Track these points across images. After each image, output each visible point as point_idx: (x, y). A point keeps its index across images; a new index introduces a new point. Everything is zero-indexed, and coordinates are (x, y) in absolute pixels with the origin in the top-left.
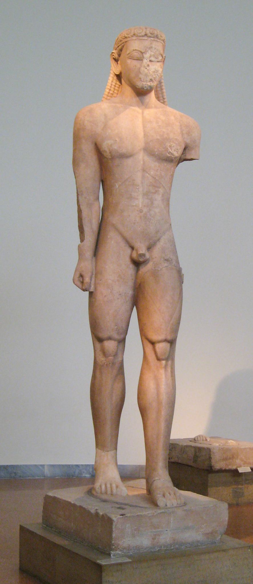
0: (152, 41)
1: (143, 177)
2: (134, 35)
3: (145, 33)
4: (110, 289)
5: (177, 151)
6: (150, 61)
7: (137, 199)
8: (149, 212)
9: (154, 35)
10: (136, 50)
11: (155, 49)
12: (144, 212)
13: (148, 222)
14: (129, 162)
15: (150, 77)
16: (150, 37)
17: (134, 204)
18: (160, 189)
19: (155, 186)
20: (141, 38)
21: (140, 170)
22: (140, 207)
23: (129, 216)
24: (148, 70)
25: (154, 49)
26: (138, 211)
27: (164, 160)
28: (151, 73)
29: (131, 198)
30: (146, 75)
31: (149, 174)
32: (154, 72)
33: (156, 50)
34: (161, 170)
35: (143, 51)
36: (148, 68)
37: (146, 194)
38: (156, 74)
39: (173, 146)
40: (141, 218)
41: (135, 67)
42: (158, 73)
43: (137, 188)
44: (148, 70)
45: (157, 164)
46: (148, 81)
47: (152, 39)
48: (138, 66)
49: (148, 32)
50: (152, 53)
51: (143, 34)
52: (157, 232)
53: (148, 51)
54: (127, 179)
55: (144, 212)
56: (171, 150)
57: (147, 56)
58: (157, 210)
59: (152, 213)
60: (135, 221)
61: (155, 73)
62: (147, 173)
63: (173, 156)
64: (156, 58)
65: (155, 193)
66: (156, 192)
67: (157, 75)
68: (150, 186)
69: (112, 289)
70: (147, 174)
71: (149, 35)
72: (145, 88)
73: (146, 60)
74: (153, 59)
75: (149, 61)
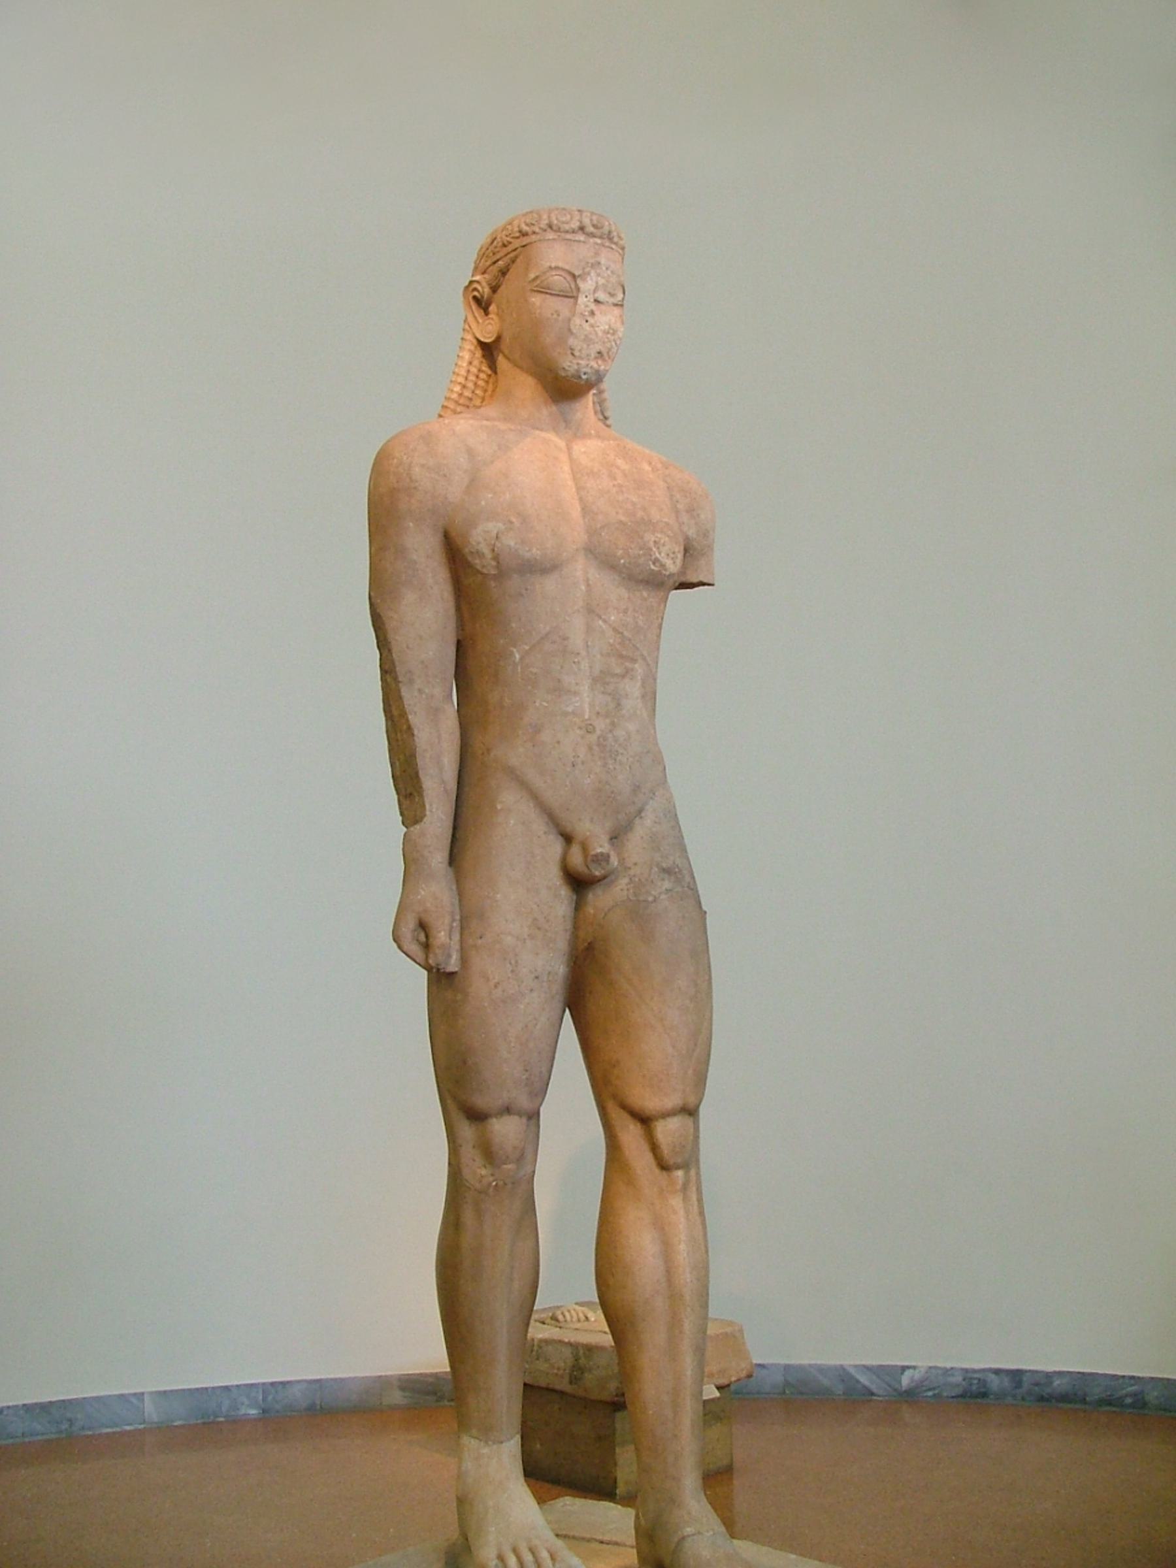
0: (597, 247)
1: (589, 629)
2: (550, 226)
3: (578, 224)
4: (510, 964)
5: (673, 558)
6: (597, 301)
7: (576, 693)
8: (611, 731)
9: (601, 230)
10: (557, 268)
11: (607, 269)
12: (598, 732)
13: (610, 762)
14: (549, 584)
15: (598, 347)
16: (592, 235)
17: (570, 709)
18: (636, 666)
19: (621, 656)
20: (568, 236)
21: (581, 610)
22: (587, 717)
23: (558, 742)
24: (592, 326)
25: (604, 268)
26: (580, 728)
27: (641, 581)
28: (600, 334)
29: (559, 690)
30: (588, 340)
31: (605, 621)
32: (608, 333)
33: (609, 272)
34: (634, 610)
35: (577, 273)
36: (591, 320)
37: (600, 680)
38: (612, 338)
39: (662, 541)
40: (590, 748)
41: (555, 316)
42: (616, 337)
43: (574, 662)
44: (592, 326)
45: (623, 592)
46: (593, 356)
47: (599, 241)
48: (565, 312)
49: (587, 221)
50: (601, 281)
51: (575, 225)
52: (636, 789)
53: (589, 274)
54: (547, 634)
55: (598, 732)
56: (660, 553)
57: (587, 285)
58: (632, 727)
59: (620, 733)
60: (574, 757)
61: (609, 336)
62: (600, 617)
63: (666, 570)
64: (612, 295)
65: (623, 676)
66: (627, 673)
67: (613, 343)
68: (608, 655)
69: (517, 962)
70: (600, 622)
71: (591, 229)
72: (584, 377)
73: (584, 296)
74: (601, 296)
75: (592, 300)
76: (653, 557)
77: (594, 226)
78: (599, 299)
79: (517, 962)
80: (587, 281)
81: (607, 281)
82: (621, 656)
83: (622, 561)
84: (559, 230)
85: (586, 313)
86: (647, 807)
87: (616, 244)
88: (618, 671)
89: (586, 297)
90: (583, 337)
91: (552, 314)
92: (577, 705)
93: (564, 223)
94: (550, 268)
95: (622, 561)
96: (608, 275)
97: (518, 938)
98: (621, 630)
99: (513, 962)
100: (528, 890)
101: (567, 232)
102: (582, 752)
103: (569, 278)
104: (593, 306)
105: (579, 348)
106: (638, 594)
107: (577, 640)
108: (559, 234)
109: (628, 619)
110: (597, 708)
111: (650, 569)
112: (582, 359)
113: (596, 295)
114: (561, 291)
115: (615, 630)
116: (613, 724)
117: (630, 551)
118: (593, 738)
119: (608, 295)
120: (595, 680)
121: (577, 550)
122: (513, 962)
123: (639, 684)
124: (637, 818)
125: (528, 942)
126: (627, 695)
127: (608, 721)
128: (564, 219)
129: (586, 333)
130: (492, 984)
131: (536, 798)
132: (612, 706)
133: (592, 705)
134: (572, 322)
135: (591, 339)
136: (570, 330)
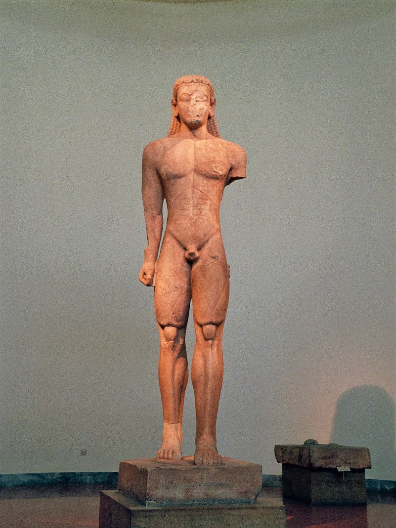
1: (193, 192)
7: (188, 210)
10: (185, 94)
14: (182, 181)
15: (197, 114)
16: (196, 82)
18: (208, 201)
20: (189, 84)
29: (183, 209)
36: (194, 107)
37: (196, 206)
40: (191, 224)
44: (195, 108)
45: (205, 181)
48: (187, 106)
55: (194, 220)
57: (193, 97)
59: (201, 220)
64: (202, 98)
69: (169, 283)
70: (197, 190)
72: (193, 123)
74: (198, 99)
76: (214, 171)
79: (169, 283)
88: (201, 203)
101: (188, 83)
102: (189, 225)
103: (188, 96)
106: (209, 181)
107: (189, 195)
115: (201, 192)
116: (199, 217)
118: (192, 222)
120: (194, 206)
121: (191, 171)
124: (206, 244)
127: (197, 217)
131: (175, 238)
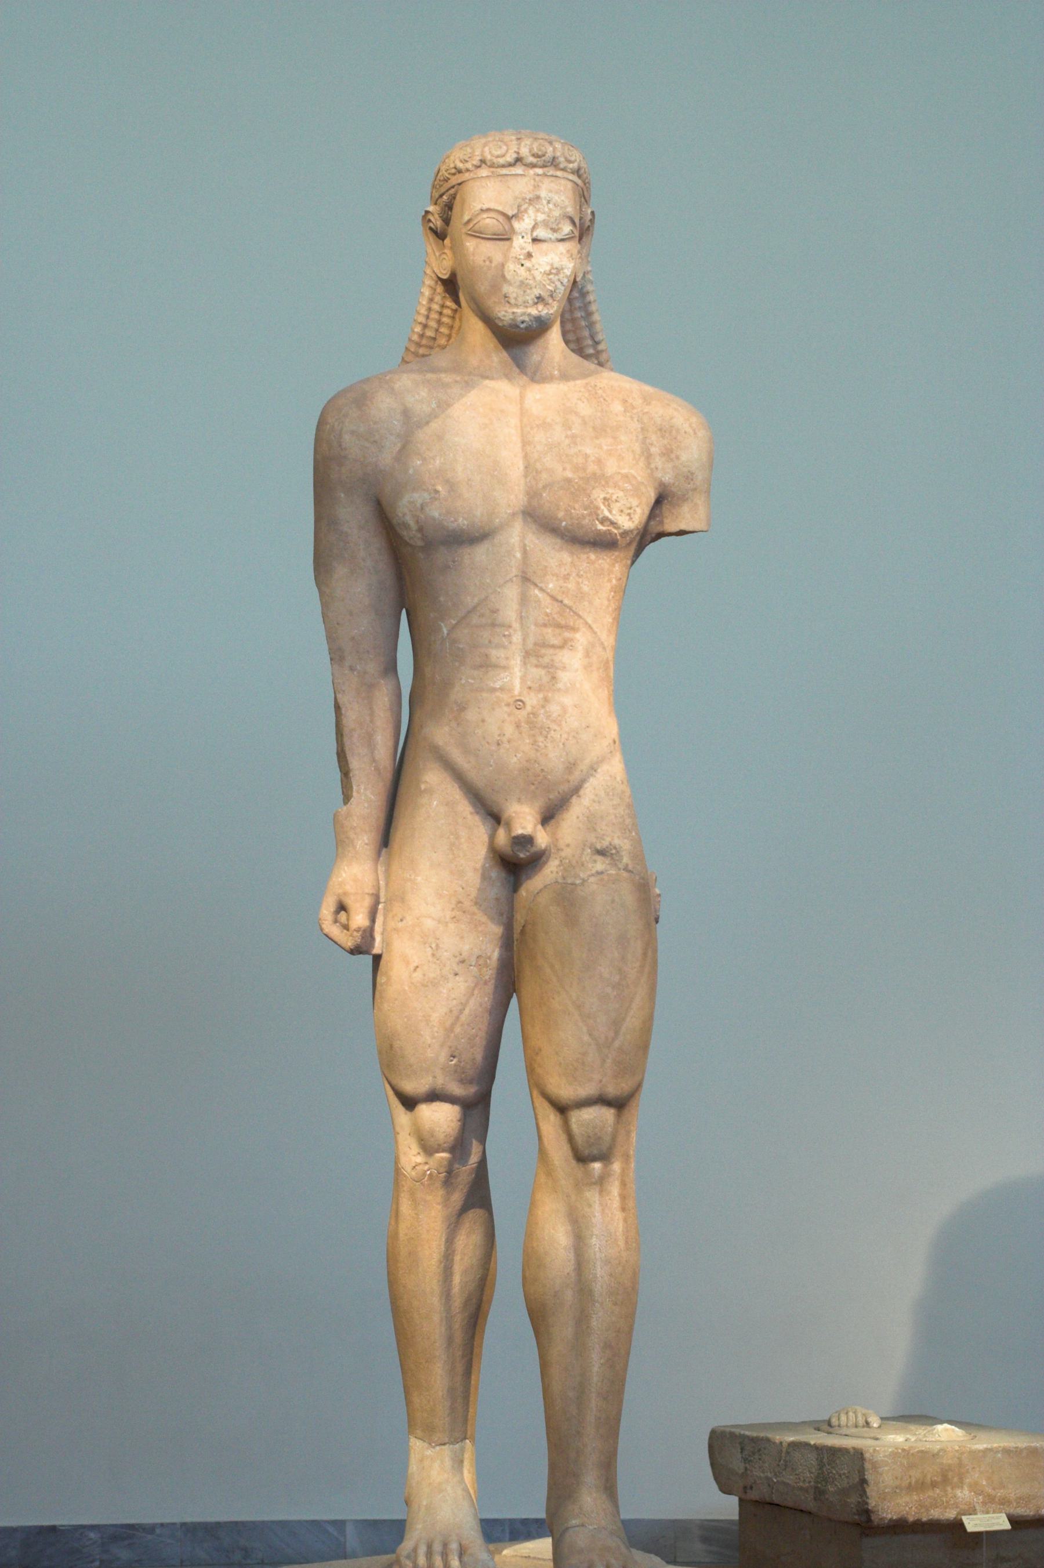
0: (537, 178)
1: (524, 600)
3: (515, 156)
6: (535, 240)
7: (505, 668)
10: (489, 210)
11: (549, 202)
15: (537, 292)
16: (533, 166)
17: (498, 685)
18: (578, 636)
20: (504, 171)
24: (529, 270)
25: (545, 202)
30: (523, 285)
31: (541, 589)
33: (551, 206)
36: (527, 264)
41: (487, 263)
43: (504, 636)
44: (529, 270)
47: (540, 171)
48: (498, 258)
50: (541, 217)
51: (510, 157)
53: (526, 211)
57: (523, 225)
61: (551, 276)
62: (536, 585)
64: (554, 230)
65: (561, 647)
70: (537, 591)
73: (520, 237)
74: (541, 233)
77: (534, 155)
78: (539, 238)
79: (437, 945)
80: (523, 220)
81: (548, 216)
82: (559, 626)
83: (564, 524)
84: (492, 166)
85: (522, 257)
86: (587, 785)
87: (564, 170)
88: (555, 641)
89: (523, 237)
90: (518, 283)
91: (484, 261)
92: (505, 680)
93: (498, 157)
94: (482, 210)
95: (564, 524)
96: (550, 210)
97: (439, 922)
98: (560, 598)
99: (434, 946)
100: (452, 873)
103: (501, 218)
104: (530, 247)
105: (515, 295)
108: (492, 169)
109: (570, 586)
110: (529, 683)
111: (596, 530)
112: (517, 306)
113: (535, 234)
114: (495, 235)
115: (554, 598)
117: (573, 511)
119: (549, 231)
120: (527, 654)
122: (434, 946)
123: (580, 654)
125: (452, 926)
126: (565, 667)
128: (499, 153)
129: (521, 279)
130: (412, 968)
132: (546, 679)
133: (523, 679)
134: (506, 267)
135: (527, 285)
136: (503, 276)
